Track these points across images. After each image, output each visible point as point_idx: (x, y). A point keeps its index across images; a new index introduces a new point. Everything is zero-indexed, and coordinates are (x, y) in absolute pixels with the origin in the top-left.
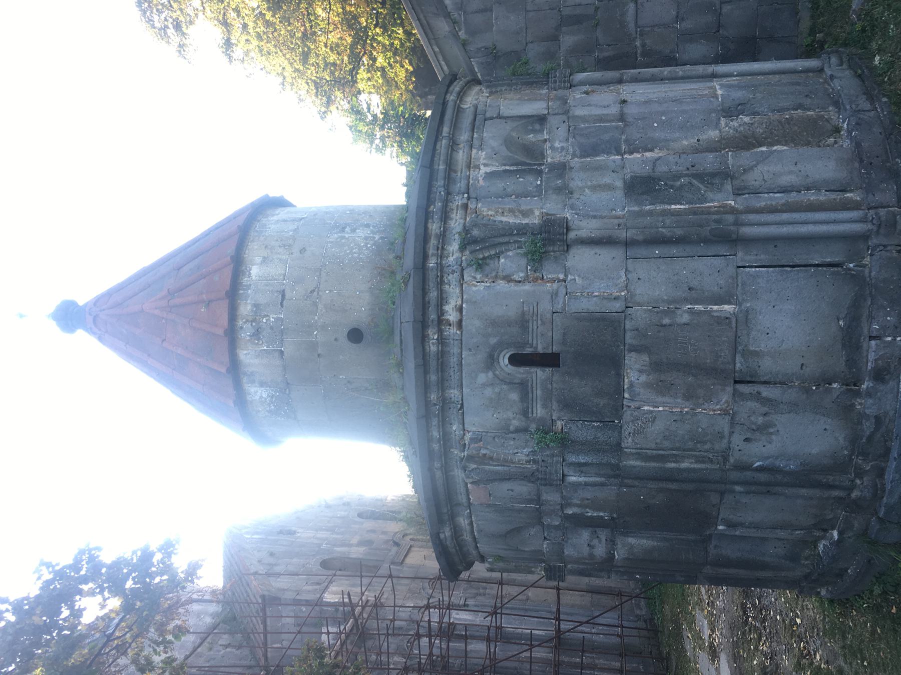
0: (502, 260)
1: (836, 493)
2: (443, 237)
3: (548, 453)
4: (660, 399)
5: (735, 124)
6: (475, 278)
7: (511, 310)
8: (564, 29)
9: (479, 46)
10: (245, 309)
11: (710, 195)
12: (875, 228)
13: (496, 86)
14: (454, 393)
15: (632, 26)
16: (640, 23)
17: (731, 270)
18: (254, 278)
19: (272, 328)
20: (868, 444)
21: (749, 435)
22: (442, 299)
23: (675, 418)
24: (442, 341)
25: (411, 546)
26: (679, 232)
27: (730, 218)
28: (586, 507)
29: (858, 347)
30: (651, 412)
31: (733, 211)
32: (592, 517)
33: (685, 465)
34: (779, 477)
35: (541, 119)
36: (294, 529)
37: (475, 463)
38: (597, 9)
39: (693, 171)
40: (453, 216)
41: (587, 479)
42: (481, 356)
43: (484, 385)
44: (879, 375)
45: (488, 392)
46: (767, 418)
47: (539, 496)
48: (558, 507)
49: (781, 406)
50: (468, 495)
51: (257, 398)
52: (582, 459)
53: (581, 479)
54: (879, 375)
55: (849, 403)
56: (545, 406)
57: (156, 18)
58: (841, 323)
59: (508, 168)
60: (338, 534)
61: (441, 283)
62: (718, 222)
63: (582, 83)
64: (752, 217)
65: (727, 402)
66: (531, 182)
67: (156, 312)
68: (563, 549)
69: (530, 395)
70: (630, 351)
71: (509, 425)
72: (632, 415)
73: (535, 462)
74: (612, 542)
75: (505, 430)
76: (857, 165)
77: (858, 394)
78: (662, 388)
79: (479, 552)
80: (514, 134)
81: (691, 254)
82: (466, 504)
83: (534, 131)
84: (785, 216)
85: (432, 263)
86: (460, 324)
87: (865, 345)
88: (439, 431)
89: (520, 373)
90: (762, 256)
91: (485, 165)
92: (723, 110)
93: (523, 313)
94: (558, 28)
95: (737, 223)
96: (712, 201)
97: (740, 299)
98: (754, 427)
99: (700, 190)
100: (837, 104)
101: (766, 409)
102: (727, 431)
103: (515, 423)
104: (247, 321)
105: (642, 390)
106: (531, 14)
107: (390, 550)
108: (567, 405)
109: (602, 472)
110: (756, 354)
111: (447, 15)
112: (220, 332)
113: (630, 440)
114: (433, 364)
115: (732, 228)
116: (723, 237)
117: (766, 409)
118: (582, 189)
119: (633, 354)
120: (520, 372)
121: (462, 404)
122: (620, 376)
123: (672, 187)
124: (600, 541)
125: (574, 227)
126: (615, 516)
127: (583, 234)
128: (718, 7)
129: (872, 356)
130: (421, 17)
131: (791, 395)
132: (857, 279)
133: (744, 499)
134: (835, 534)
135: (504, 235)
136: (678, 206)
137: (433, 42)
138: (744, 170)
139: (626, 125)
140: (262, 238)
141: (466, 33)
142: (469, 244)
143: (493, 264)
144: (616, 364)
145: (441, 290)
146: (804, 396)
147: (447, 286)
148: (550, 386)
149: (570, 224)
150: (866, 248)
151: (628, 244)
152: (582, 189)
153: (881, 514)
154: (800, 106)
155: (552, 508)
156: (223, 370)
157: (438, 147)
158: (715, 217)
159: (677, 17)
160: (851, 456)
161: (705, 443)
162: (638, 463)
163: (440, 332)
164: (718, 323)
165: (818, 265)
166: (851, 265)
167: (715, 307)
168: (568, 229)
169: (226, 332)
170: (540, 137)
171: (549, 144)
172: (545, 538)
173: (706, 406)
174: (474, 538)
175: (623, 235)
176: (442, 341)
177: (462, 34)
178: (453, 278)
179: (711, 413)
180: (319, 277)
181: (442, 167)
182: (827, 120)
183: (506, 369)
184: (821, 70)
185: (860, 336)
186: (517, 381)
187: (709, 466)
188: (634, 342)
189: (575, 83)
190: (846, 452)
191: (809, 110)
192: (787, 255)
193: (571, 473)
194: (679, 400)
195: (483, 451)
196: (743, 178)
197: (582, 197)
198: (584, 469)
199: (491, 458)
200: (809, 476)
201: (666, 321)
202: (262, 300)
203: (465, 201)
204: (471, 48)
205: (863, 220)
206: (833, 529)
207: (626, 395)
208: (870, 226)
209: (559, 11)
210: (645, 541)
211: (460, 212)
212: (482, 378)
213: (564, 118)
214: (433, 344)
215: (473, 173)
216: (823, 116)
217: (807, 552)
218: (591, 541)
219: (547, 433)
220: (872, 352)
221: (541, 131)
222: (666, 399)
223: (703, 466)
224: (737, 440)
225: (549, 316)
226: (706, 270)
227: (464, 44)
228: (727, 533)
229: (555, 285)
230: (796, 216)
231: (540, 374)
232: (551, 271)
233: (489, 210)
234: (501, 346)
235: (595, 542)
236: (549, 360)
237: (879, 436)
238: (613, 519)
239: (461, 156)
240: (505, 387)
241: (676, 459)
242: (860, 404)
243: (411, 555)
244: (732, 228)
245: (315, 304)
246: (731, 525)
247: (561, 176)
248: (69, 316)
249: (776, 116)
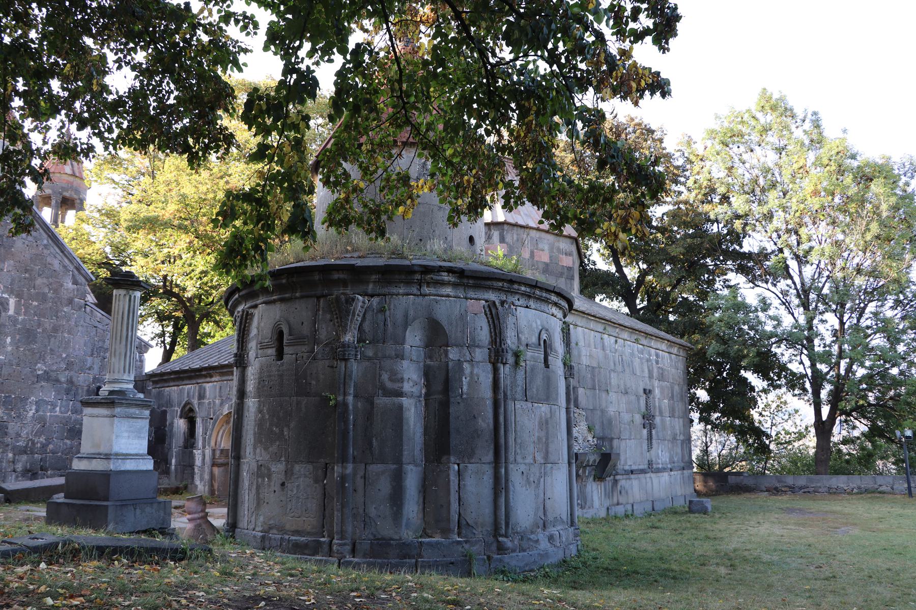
14: (532, 303)
47: (478, 346)
50: (476, 299)
56: (532, 357)
74: (412, 396)
78: (541, 424)
126: (464, 396)
212: (539, 323)
224: (523, 468)
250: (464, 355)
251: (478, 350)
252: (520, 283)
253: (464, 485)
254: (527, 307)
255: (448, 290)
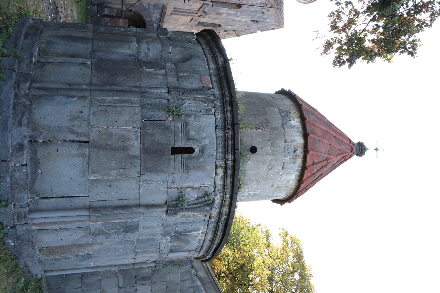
0: (196, 196)
1: (38, 85)
2: (222, 206)
3: (175, 104)
4: (123, 132)
5: (86, 252)
6: (209, 188)
7: (193, 174)
8: (150, 275)
9: (186, 267)
10: (299, 161)
11: (100, 226)
12: (27, 216)
13: (188, 260)
15: (120, 277)
16: (117, 278)
17: (91, 195)
18: (294, 175)
19: (289, 153)
20: (23, 110)
21: (81, 115)
22: (224, 179)
23: (116, 123)
24: (225, 160)
25: (198, 11)
26: (116, 212)
27: (93, 218)
28: (155, 74)
29: (31, 159)
30: (127, 126)
31: (91, 221)
32: (152, 68)
33: (110, 98)
34: (66, 93)
35: (171, 251)
36: (251, 23)
37: (210, 99)
38: (136, 283)
39: (108, 236)
40: (216, 214)
41: (157, 91)
42: (207, 152)
43: (206, 138)
44: (21, 147)
45: (204, 135)
46: (72, 124)
47: (178, 80)
48: (168, 74)
49: (66, 130)
50: (211, 80)
51: (296, 120)
52: (159, 101)
53: (160, 91)
54: (21, 147)
55: (34, 132)
56: (178, 128)
57: (296, 247)
58: (40, 171)
59: (189, 233)
60: (232, 19)
61: (224, 186)
62: (98, 217)
63: (151, 263)
64: (83, 219)
65: (92, 132)
66: (180, 229)
67: (332, 157)
68: (162, 48)
69: (185, 134)
70: (138, 156)
71: (194, 118)
72: (137, 124)
73: (182, 99)
74: (138, 51)
75: (196, 115)
76: (34, 240)
77: (30, 137)
78: (123, 138)
79: (201, 46)
80: (184, 245)
81: (109, 201)
82: (212, 76)
83: (175, 246)
84: (68, 220)
85: (228, 195)
86: (216, 168)
87: (29, 161)
88: (227, 116)
89: (190, 145)
90: (77, 201)
91: (199, 234)
92: (91, 257)
93: (188, 173)
94: (152, 275)
95: (90, 216)
96: (100, 224)
97: (87, 182)
98: (78, 119)
99: (105, 228)
100: (40, 261)
101: (74, 128)
102: (91, 116)
103: (191, 119)
104: (299, 156)
105: (132, 137)
106: (164, 280)
107: (208, 10)
108: (168, 128)
109: (150, 95)
110: (79, 156)
111: (199, 278)
112: (311, 152)
113: (137, 111)
114: (230, 149)
115: (92, 214)
116: (94, 209)
117: (74, 128)
118: (158, 227)
119: (137, 155)
120: (189, 145)
121: (216, 128)
122: (143, 144)
123: (117, 229)
124: (144, 51)
125: (164, 213)
126: (141, 69)
127: (159, 210)
128: (83, 286)
129: (25, 156)
130: (211, 277)
131: (62, 136)
132: (33, 191)
133: (80, 80)
134: (34, 60)
135: (196, 208)
136: (115, 221)
137: (206, 268)
138: (85, 236)
139: (134, 250)
140: (288, 190)
141: (192, 272)
142: (212, 204)
143: (200, 195)
144: (145, 150)
145: (224, 182)
146: (55, 136)
147: (221, 184)
148: (176, 138)
149: (165, 214)
150: (30, 206)
151: (139, 206)
152: (158, 227)
153: (14, 73)
154: (57, 260)
155: (171, 73)
156: (310, 134)
157: (219, 241)
158: (100, 218)
159: (100, 281)
160: (31, 105)
161: (101, 110)
162: (132, 99)
163: (226, 163)
164: (97, 170)
165: (52, 198)
166: (36, 198)
167: (99, 178)
168: (167, 211)
169: (308, 152)
170: (172, 244)
171: (168, 241)
172: (171, 53)
173: (102, 130)
174: (205, 55)
175: (142, 210)
176: (225, 160)
177: (193, 271)
178: (219, 187)
179: (99, 126)
180: (267, 176)
181: (219, 233)
182: (45, 254)
183: (197, 147)
184: (45, 272)
185: (31, 166)
186: (191, 141)
187: (99, 98)
188: (136, 160)
189: (154, 263)
190: (34, 106)
191: (53, 259)
192: (67, 204)
193: (165, 94)
194: (114, 132)
195: (206, 105)
196: (85, 234)
197: (158, 223)
198: (158, 96)
199: (202, 101)
200: (51, 93)
201: (121, 171)
202: (292, 165)
203: (210, 220)
204: (189, 266)
205: (32, 219)
206: (35, 62)
207: (139, 134)
208: (29, 217)
209: (152, 282)
210: (122, 52)
211: (212, 216)
212: (207, 142)
213: (161, 252)
214: (230, 159)
215: (205, 230)
216: (46, 256)
217: (43, 46)
218: (148, 52)
219: (177, 114)
220: (25, 158)
221: (172, 246)
222: (120, 132)
223: (101, 98)
224: (86, 112)
225: (176, 172)
226: (102, 195)
227: (193, 267)
228: (86, 60)
229: (172, 186)
230: (63, 220)
231: (180, 144)
232: (174, 193)
233: (200, 217)
234: (198, 157)
235: (146, 51)
236: (176, 151)
237: (19, 116)
238: (141, 67)
239: (210, 236)
240: (196, 137)
241: (114, 101)
242: (29, 132)
243: (199, 7)
244: (92, 214)
245: (270, 164)
246: (84, 64)
247: (166, 231)
248: (360, 150)
249: (68, 255)
250: (170, 71)
251: (175, 79)
252: (232, 111)
253: (76, 65)
254: (216, 126)
255: (212, 66)
